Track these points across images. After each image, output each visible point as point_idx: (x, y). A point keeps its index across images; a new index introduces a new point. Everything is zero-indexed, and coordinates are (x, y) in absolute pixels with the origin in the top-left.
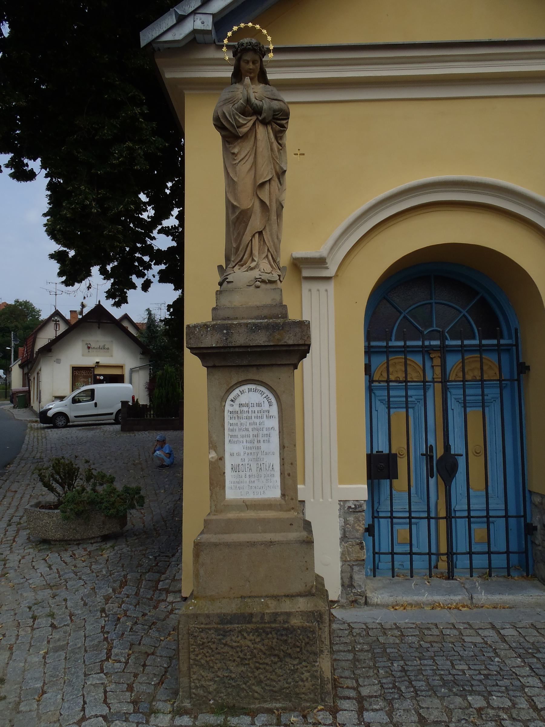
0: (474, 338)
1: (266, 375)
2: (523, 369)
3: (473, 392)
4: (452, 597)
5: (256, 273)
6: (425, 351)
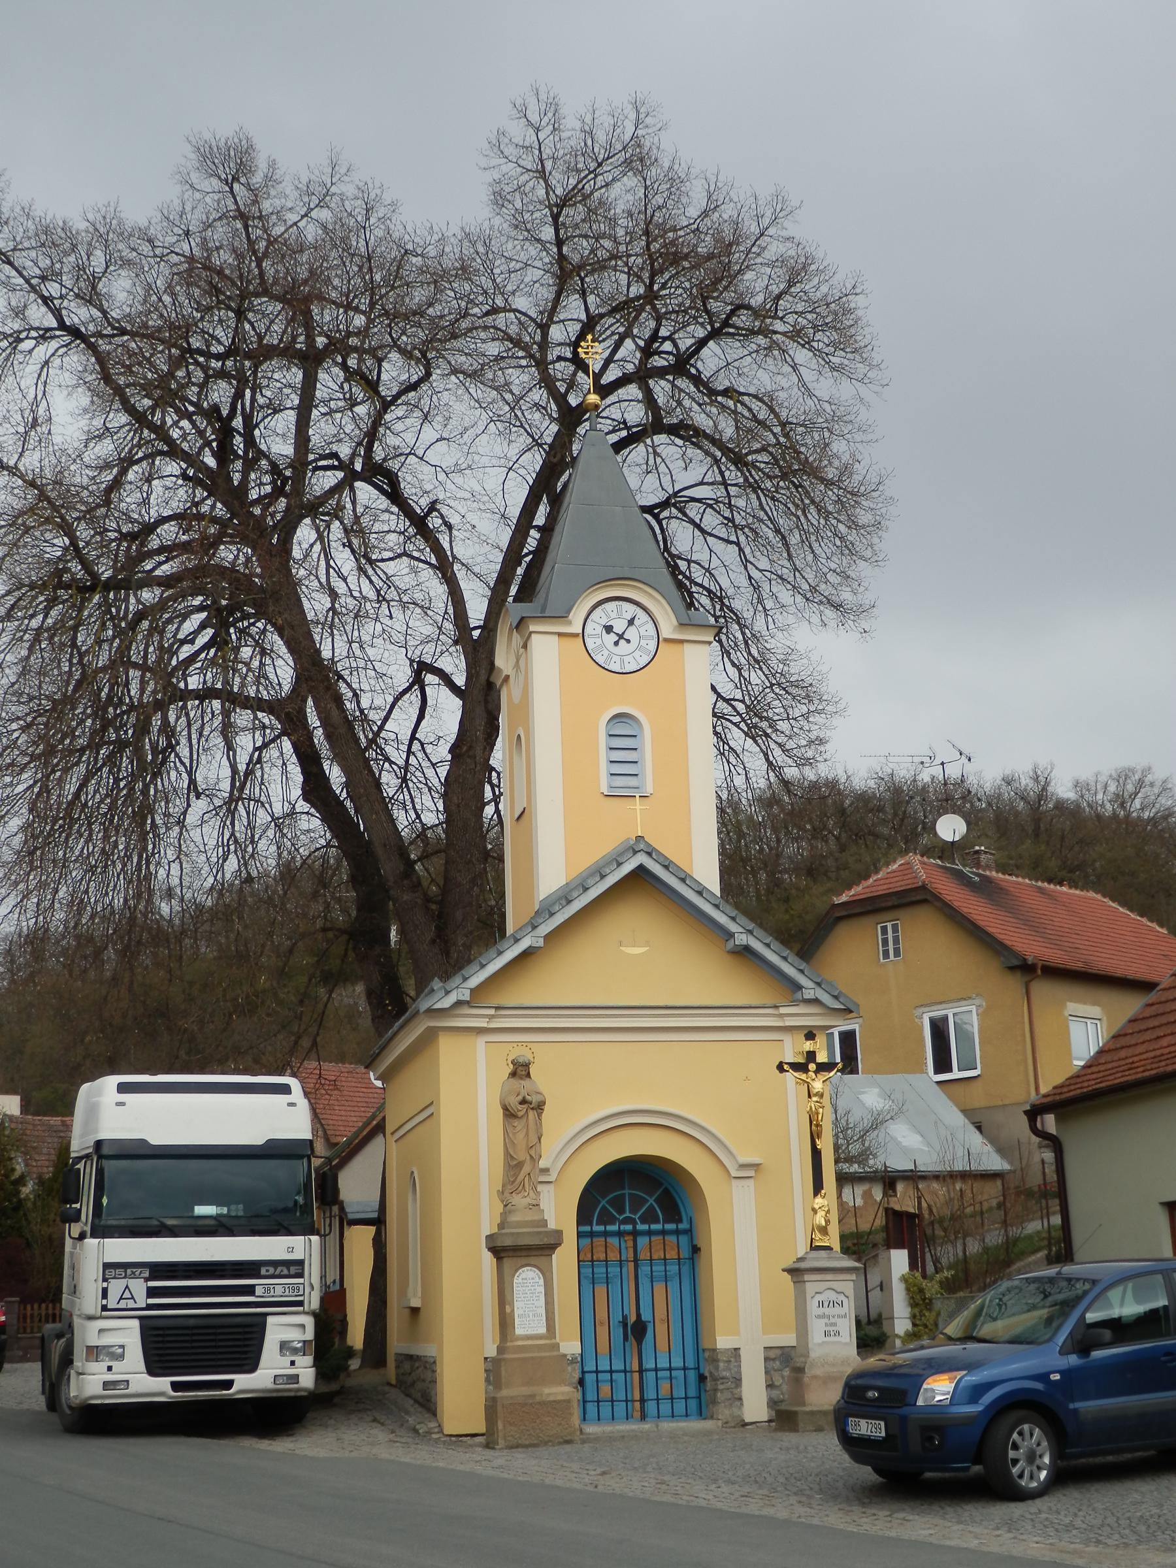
0: (657, 1222)
1: (533, 1260)
2: (696, 1250)
3: (659, 1268)
5: (528, 1200)
6: (620, 1234)
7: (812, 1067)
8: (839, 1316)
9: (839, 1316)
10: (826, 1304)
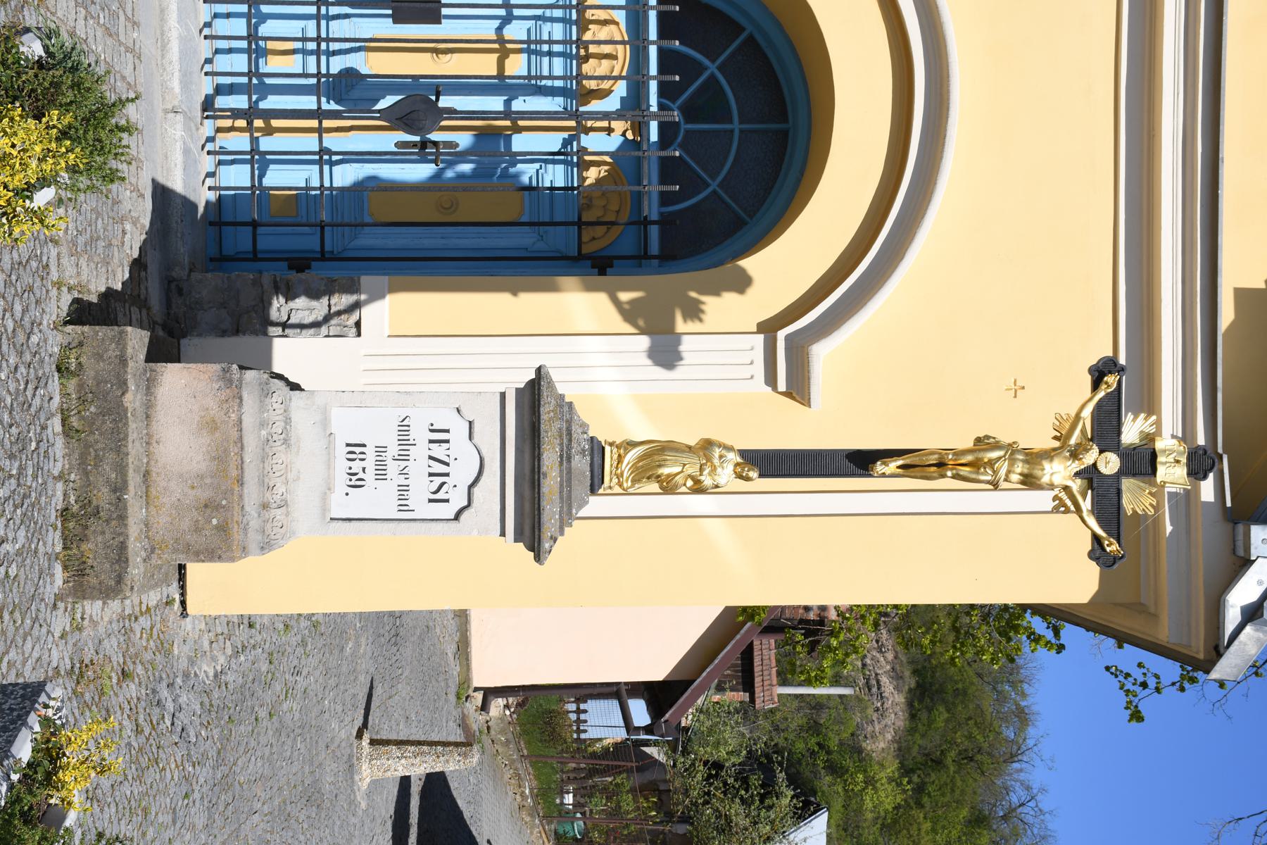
4: (177, 74)
7: (1110, 464)
8: (403, 489)
9: (403, 489)
10: (439, 451)
